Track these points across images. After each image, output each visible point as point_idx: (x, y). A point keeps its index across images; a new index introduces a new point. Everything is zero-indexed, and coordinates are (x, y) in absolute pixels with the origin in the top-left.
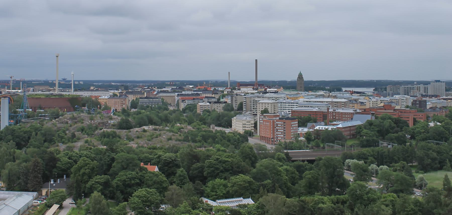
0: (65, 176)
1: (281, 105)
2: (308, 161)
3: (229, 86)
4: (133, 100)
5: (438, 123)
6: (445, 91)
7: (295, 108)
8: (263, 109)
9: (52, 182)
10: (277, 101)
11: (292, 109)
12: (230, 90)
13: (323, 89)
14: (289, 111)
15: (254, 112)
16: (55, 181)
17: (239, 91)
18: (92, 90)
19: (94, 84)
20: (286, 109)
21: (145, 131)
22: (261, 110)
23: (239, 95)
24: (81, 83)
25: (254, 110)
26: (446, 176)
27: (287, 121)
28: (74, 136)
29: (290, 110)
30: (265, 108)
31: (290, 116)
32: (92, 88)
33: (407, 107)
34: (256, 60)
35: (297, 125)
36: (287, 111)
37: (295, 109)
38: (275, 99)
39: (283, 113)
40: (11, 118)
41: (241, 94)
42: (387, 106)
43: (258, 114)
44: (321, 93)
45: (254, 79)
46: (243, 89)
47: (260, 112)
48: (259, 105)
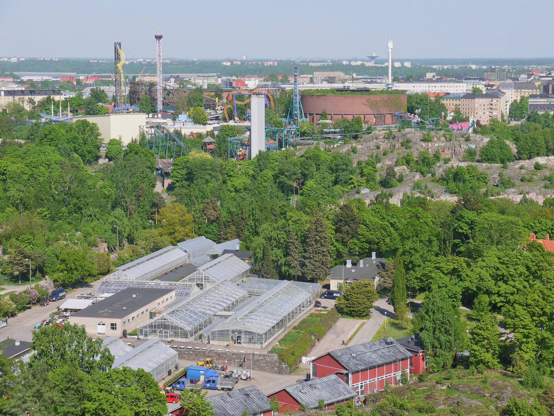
0: (374, 254)
4: (515, 101)
9: (349, 265)
16: (354, 264)
18: (430, 81)
19: (434, 67)
21: (537, 167)
24: (408, 64)
28: (390, 173)
32: (429, 75)
40: (270, 135)
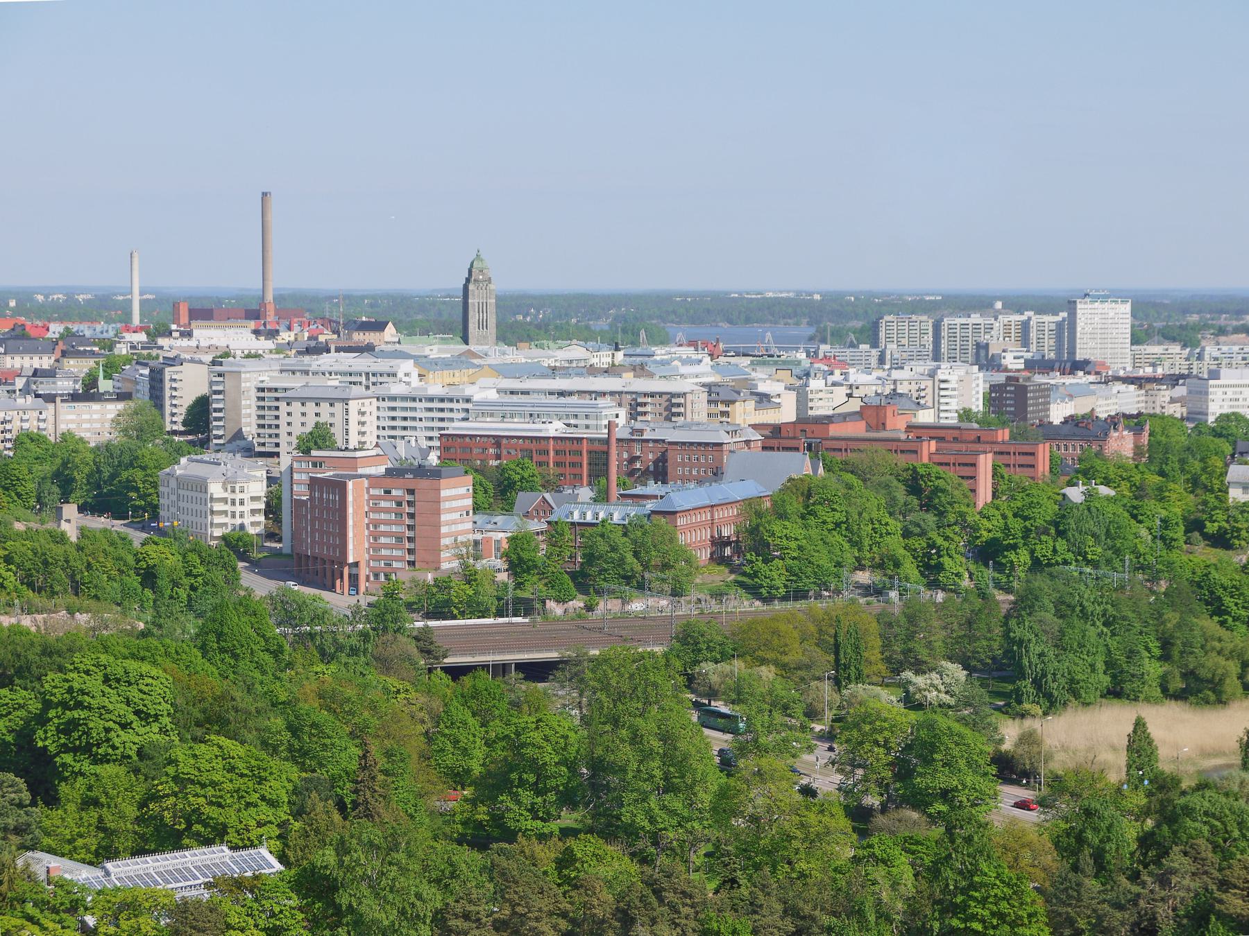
1: (394, 409)
2: (520, 666)
3: (136, 320)
5: (1104, 490)
6: (1132, 344)
7: (457, 424)
8: (308, 429)
10: (369, 393)
11: (443, 429)
12: (142, 337)
13: (586, 336)
14: (431, 438)
15: (264, 444)
17: (185, 342)
20: (415, 428)
22: (297, 430)
23: (192, 361)
25: (268, 431)
26: (1139, 725)
27: (423, 484)
29: (436, 434)
30: (317, 424)
31: (433, 459)
33: (966, 415)
34: (264, 194)
35: (469, 502)
36: (422, 434)
37: (457, 427)
38: (363, 379)
39: (399, 443)
41: (197, 357)
42: (873, 413)
43: (282, 450)
44: (576, 352)
45: (252, 283)
46: (208, 336)
47: (295, 441)
48: (289, 409)
